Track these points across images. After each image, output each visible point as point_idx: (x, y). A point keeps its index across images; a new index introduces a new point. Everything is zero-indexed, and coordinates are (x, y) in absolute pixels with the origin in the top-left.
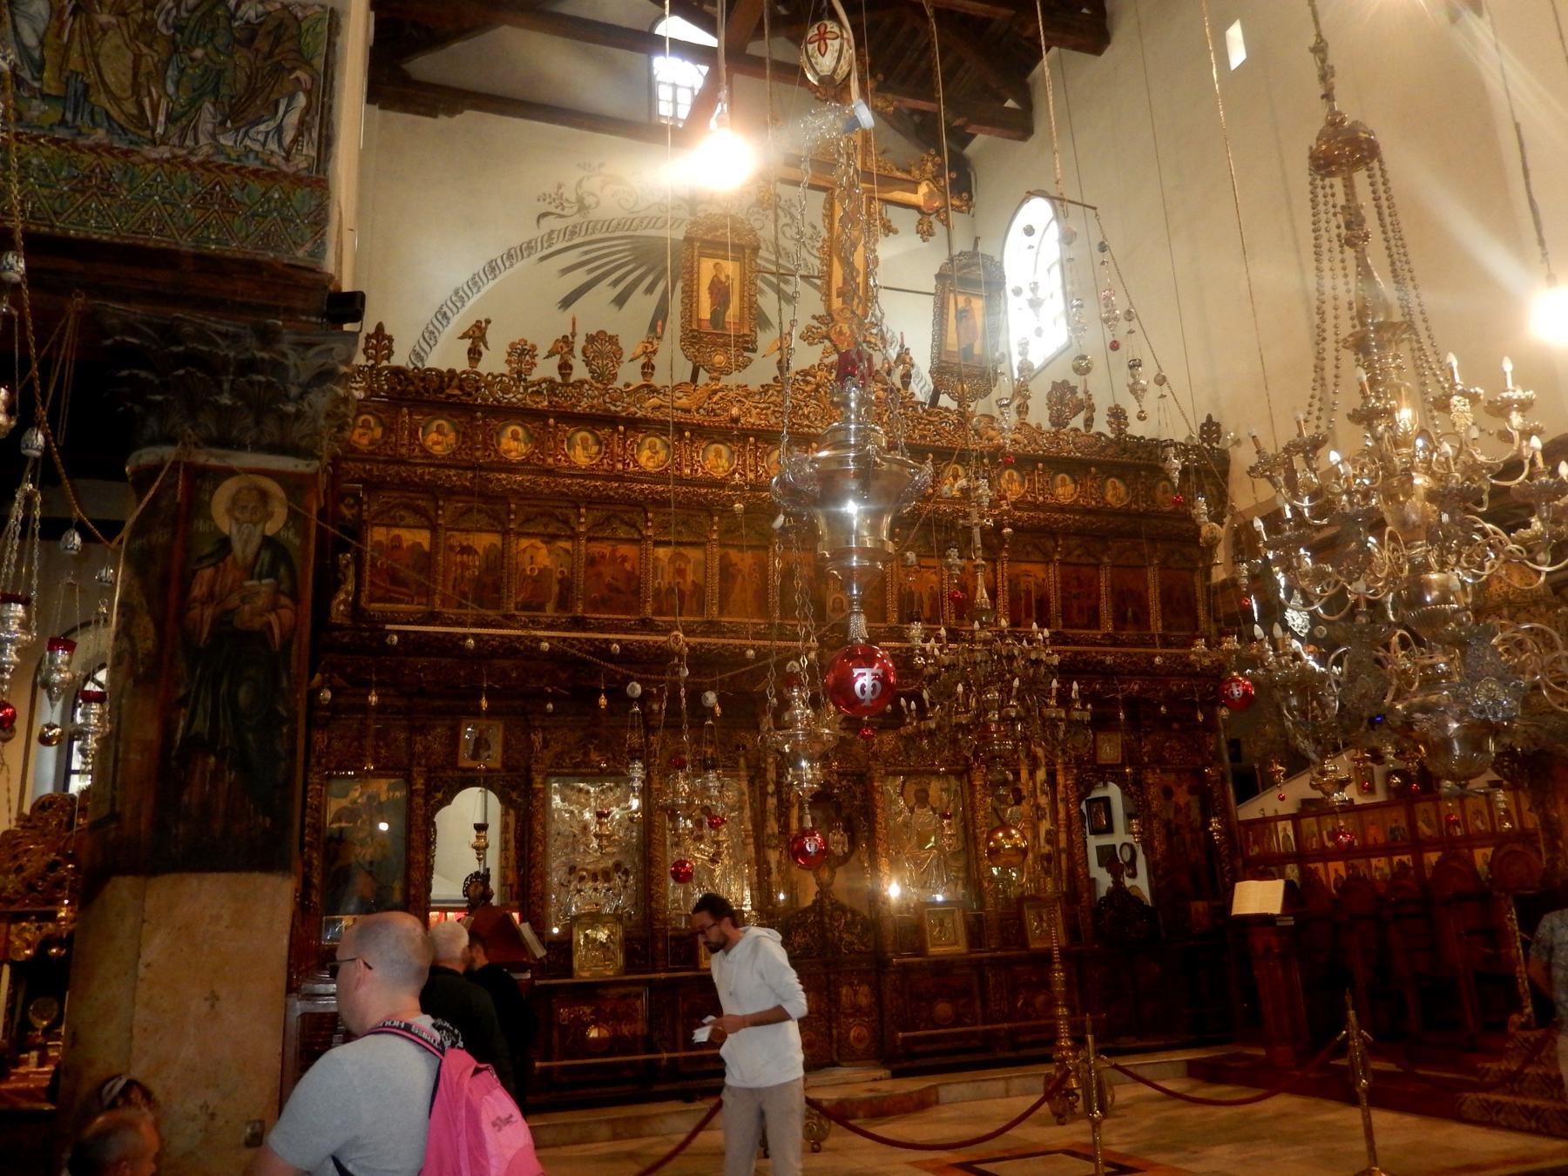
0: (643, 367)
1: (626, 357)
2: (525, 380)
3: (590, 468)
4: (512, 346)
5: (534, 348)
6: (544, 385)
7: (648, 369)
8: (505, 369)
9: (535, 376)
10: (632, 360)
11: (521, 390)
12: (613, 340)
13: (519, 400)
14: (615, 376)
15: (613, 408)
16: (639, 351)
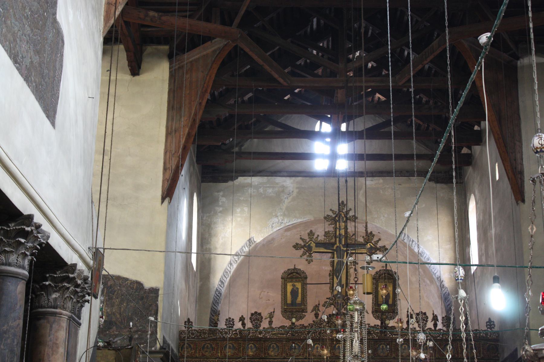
0: (269, 322)
1: (264, 318)
2: (232, 330)
3: (253, 355)
4: (227, 320)
5: (233, 319)
6: (238, 331)
7: (271, 322)
8: (225, 327)
9: (235, 327)
10: (265, 319)
11: (231, 333)
12: (260, 314)
13: (231, 336)
14: (260, 325)
15: (259, 336)
16: (268, 316)
